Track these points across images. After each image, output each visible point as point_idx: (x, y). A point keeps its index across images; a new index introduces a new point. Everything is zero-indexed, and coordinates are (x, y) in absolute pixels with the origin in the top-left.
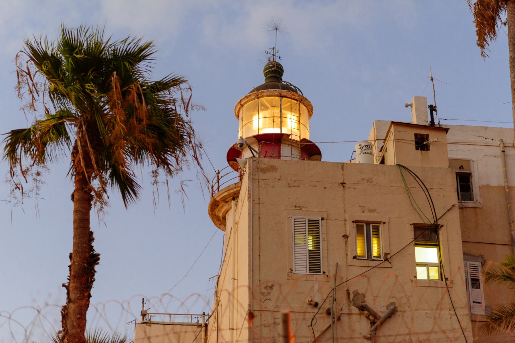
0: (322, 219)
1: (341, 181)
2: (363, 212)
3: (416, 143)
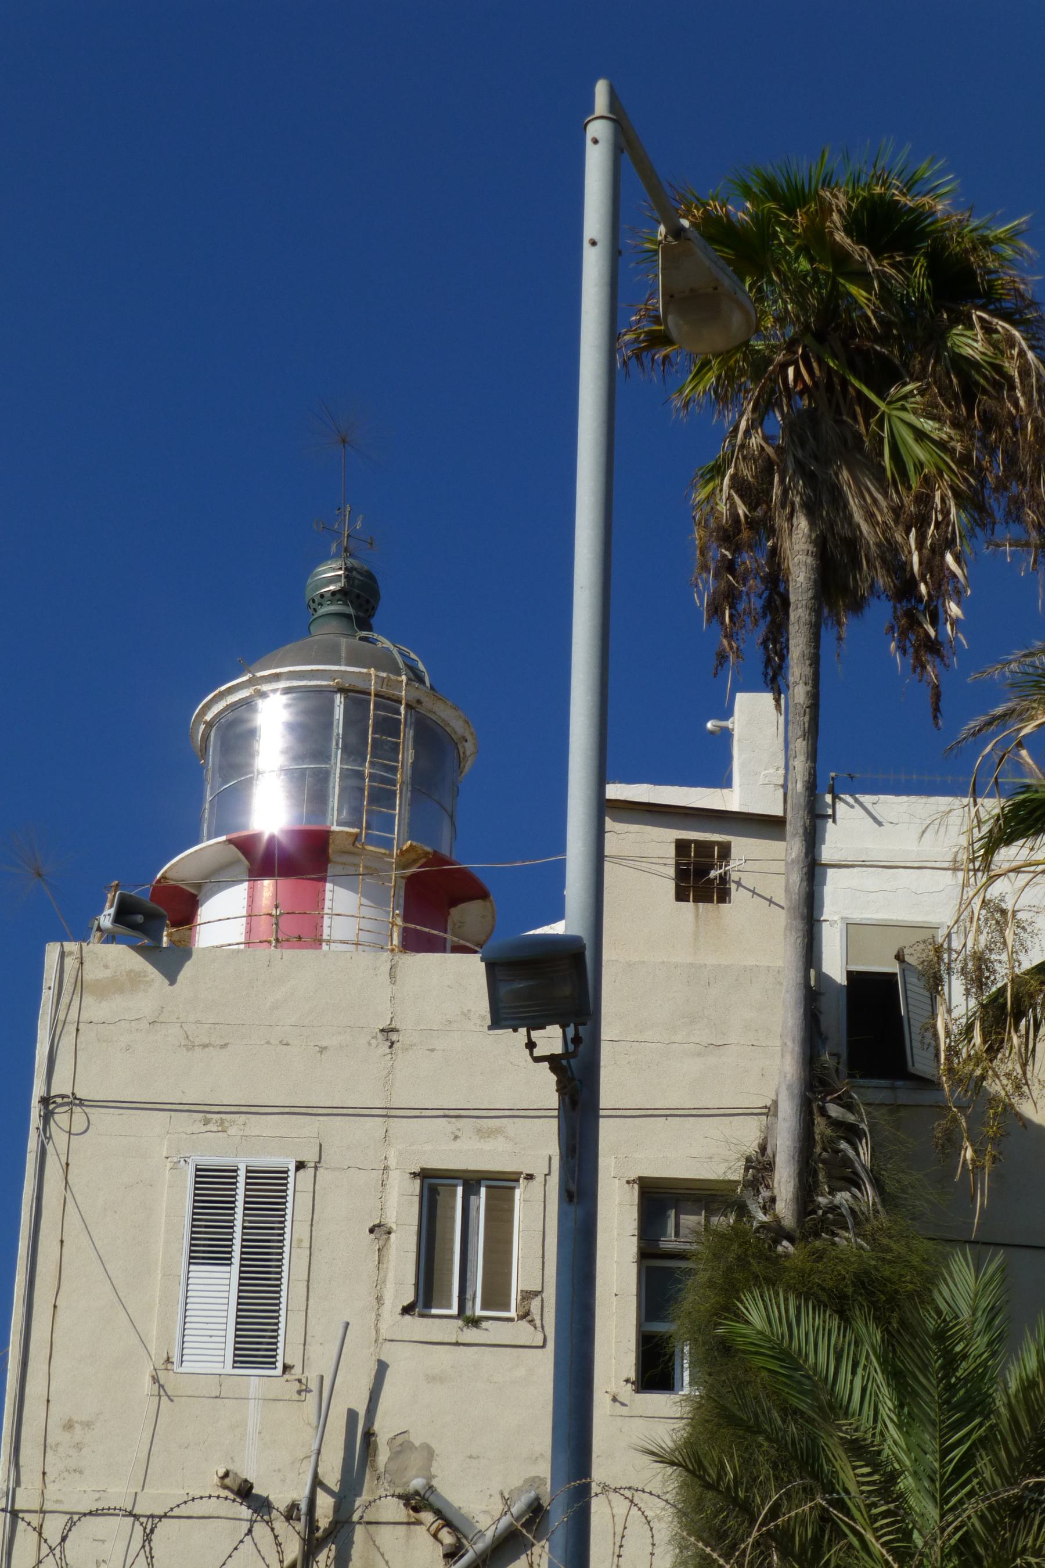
0: (300, 1166)
1: (384, 1024)
2: (456, 1137)
3: (681, 875)
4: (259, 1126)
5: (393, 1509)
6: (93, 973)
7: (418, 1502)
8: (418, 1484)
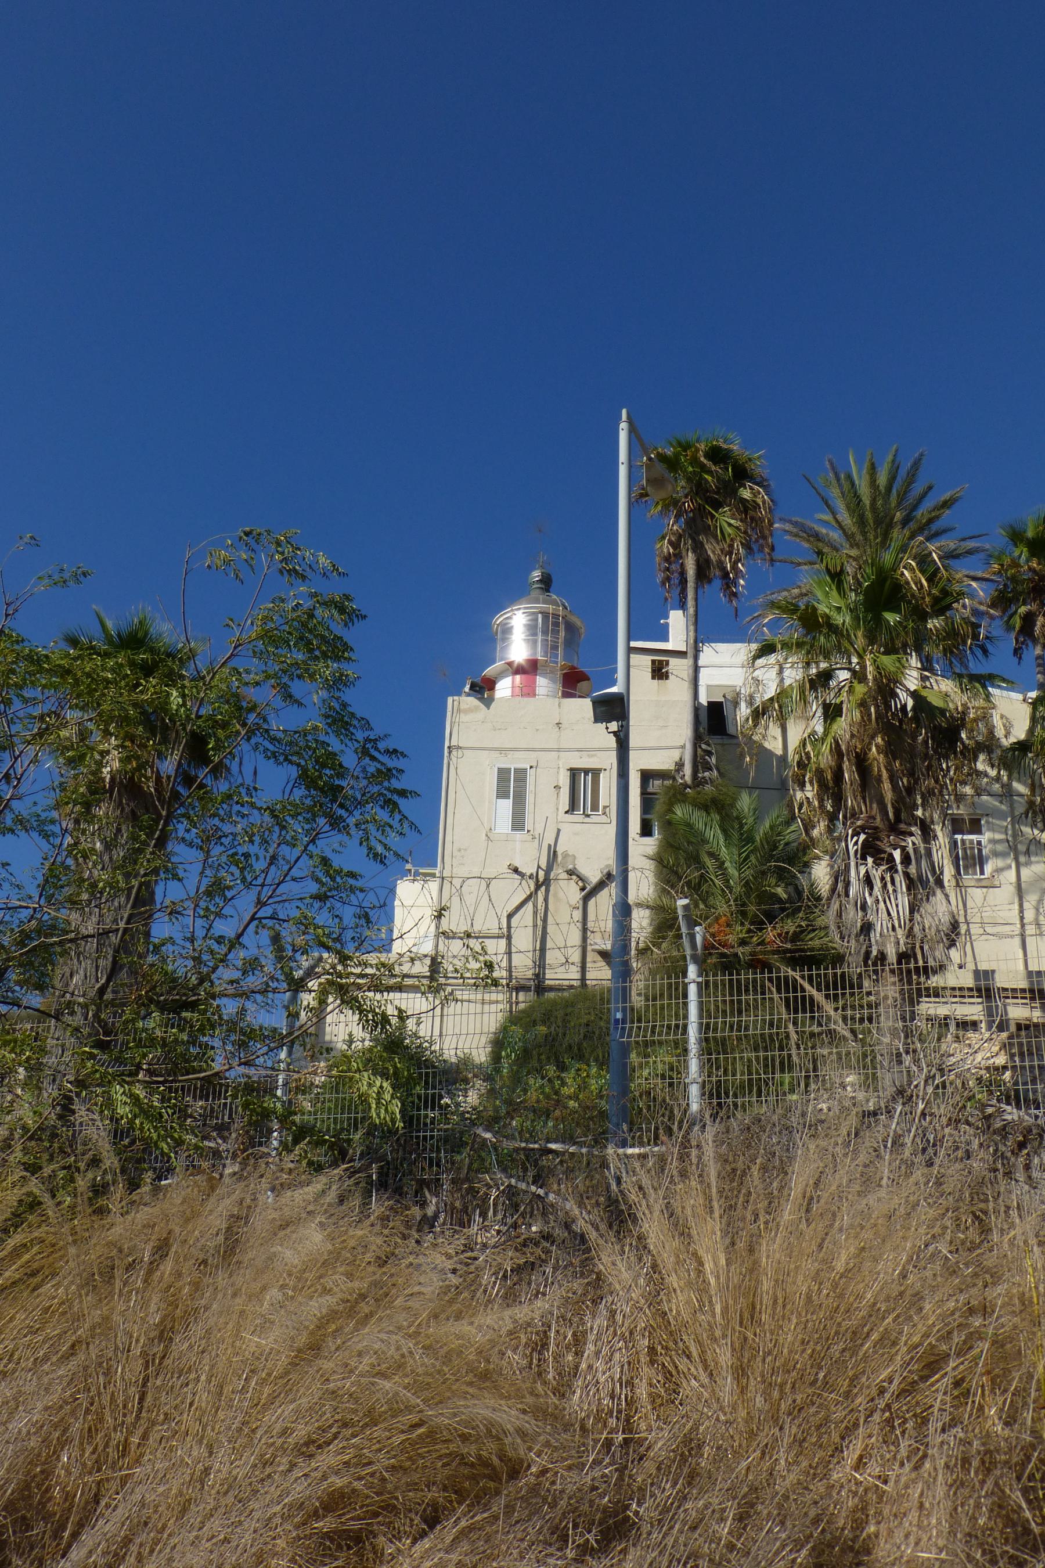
3: (653, 671)
4: (517, 755)
5: (565, 876)
6: (463, 706)
8: (571, 867)
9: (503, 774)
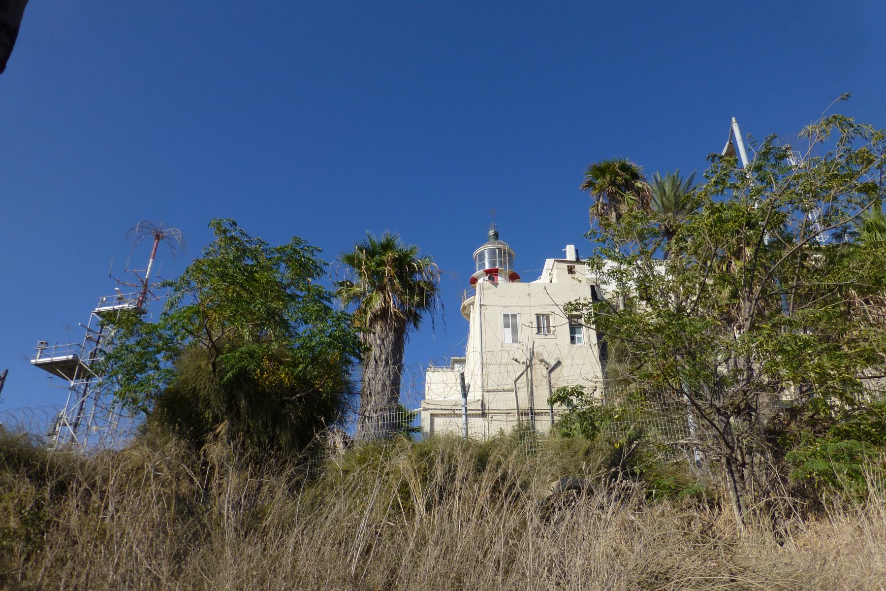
7: (542, 361)
9: (506, 317)
